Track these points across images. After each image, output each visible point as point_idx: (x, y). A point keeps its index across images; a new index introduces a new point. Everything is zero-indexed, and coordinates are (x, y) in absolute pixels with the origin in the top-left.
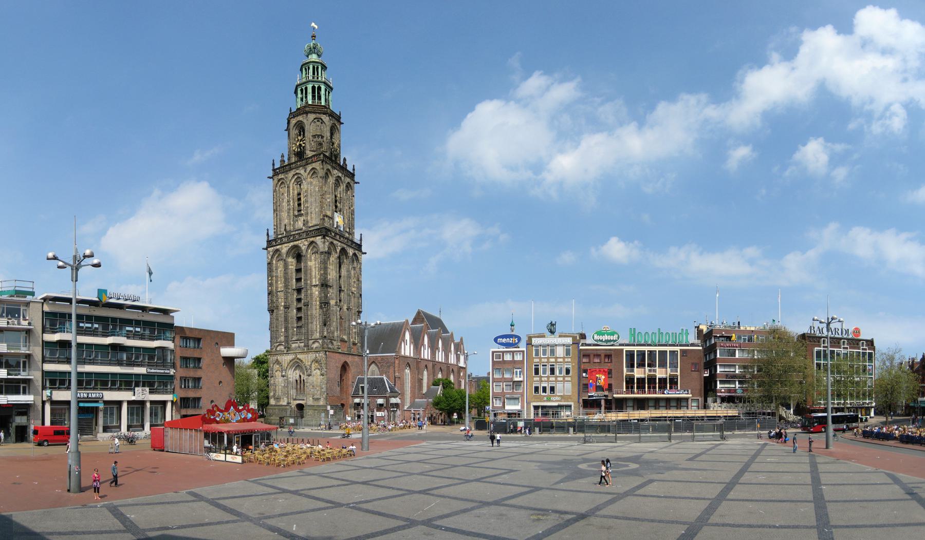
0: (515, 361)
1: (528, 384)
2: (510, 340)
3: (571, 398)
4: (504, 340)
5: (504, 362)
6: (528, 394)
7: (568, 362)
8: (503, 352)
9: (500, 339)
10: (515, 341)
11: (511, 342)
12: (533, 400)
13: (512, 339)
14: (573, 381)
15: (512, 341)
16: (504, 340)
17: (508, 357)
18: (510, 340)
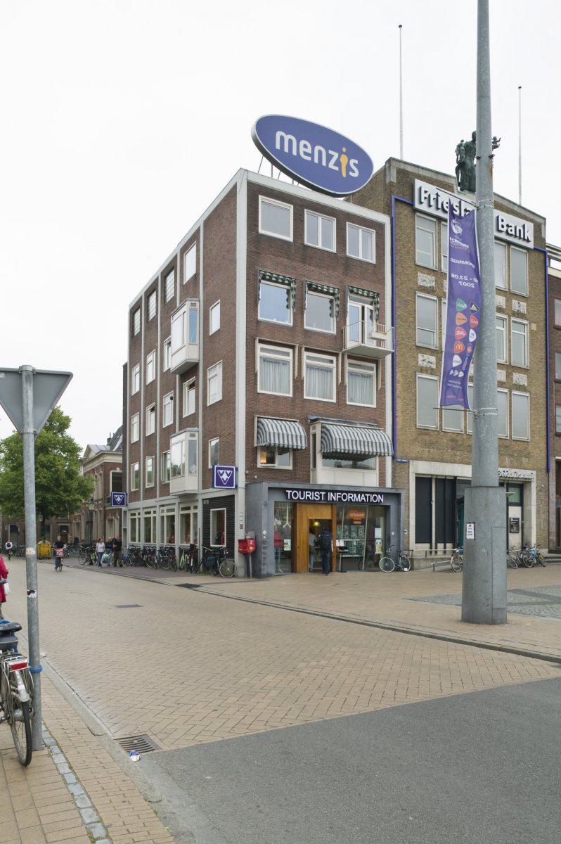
0: (348, 259)
1: (399, 376)
2: (329, 157)
3: (528, 455)
4: (303, 148)
5: (299, 251)
6: (399, 420)
7: (518, 314)
8: (301, 206)
9: (287, 137)
10: (349, 169)
11: (331, 165)
12: (417, 449)
13: (336, 155)
14: (533, 389)
15: (338, 163)
16: (303, 148)
17: (320, 234)
18: (329, 157)
